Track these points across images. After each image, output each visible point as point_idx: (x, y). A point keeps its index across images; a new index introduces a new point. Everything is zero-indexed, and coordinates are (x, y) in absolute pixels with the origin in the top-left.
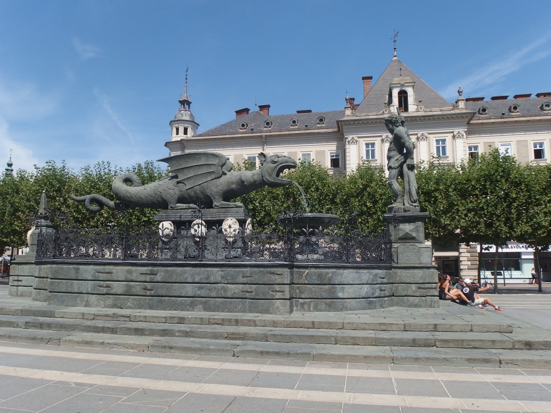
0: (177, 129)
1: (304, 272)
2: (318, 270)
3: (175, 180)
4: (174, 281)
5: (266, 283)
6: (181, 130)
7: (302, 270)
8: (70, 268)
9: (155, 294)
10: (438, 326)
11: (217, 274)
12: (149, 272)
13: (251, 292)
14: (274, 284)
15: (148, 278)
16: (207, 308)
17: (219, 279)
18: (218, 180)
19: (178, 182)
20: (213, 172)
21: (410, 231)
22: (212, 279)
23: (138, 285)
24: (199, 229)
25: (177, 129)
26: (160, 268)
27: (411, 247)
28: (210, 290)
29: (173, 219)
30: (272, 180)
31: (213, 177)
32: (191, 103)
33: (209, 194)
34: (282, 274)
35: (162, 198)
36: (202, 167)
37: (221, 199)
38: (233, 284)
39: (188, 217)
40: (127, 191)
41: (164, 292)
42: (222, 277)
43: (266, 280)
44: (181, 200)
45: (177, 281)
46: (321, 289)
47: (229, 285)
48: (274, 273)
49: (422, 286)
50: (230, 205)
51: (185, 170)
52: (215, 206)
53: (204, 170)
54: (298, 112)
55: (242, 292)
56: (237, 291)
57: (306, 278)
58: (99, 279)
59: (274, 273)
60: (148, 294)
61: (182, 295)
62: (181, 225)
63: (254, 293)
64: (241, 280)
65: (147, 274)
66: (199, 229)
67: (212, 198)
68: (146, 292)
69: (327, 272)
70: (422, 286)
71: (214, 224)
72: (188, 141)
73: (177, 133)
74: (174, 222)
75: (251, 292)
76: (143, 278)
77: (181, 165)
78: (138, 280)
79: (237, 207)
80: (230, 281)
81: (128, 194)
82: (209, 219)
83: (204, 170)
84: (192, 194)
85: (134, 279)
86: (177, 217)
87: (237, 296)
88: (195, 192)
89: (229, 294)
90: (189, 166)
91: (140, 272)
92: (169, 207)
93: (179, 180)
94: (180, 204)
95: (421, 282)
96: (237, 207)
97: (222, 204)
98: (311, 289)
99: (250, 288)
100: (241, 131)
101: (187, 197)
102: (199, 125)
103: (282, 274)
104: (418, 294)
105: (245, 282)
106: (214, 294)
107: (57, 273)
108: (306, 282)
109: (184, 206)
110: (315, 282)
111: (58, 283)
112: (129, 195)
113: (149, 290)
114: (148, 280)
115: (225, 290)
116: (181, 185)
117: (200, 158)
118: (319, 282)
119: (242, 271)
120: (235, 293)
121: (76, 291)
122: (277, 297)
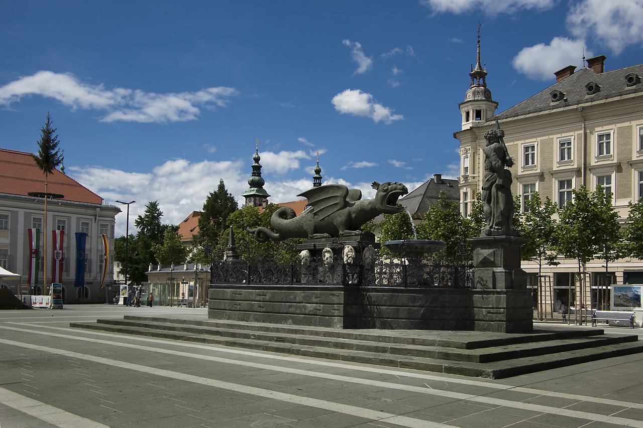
0: (468, 113)
4: (275, 301)
9: (266, 311)
10: (416, 340)
12: (261, 294)
13: (320, 310)
16: (295, 322)
21: (488, 255)
22: (297, 300)
25: (468, 113)
27: (486, 272)
28: (296, 307)
29: (309, 248)
32: (486, 74)
34: (339, 296)
37: (344, 228)
41: (269, 309)
42: (304, 298)
44: (317, 230)
48: (334, 295)
49: (492, 310)
50: (351, 233)
55: (315, 309)
56: (312, 309)
59: (334, 295)
60: (262, 311)
61: (281, 312)
62: (316, 253)
64: (314, 300)
65: (261, 295)
68: (260, 309)
70: (492, 310)
71: (337, 252)
73: (467, 120)
74: (310, 251)
75: (320, 310)
76: (258, 298)
78: (256, 300)
80: (308, 301)
87: (311, 313)
89: (307, 312)
92: (309, 237)
95: (490, 306)
100: (552, 104)
103: (339, 296)
104: (487, 318)
105: (318, 302)
106: (298, 311)
114: (261, 300)
115: (305, 308)
121: (223, 308)
122: (336, 314)
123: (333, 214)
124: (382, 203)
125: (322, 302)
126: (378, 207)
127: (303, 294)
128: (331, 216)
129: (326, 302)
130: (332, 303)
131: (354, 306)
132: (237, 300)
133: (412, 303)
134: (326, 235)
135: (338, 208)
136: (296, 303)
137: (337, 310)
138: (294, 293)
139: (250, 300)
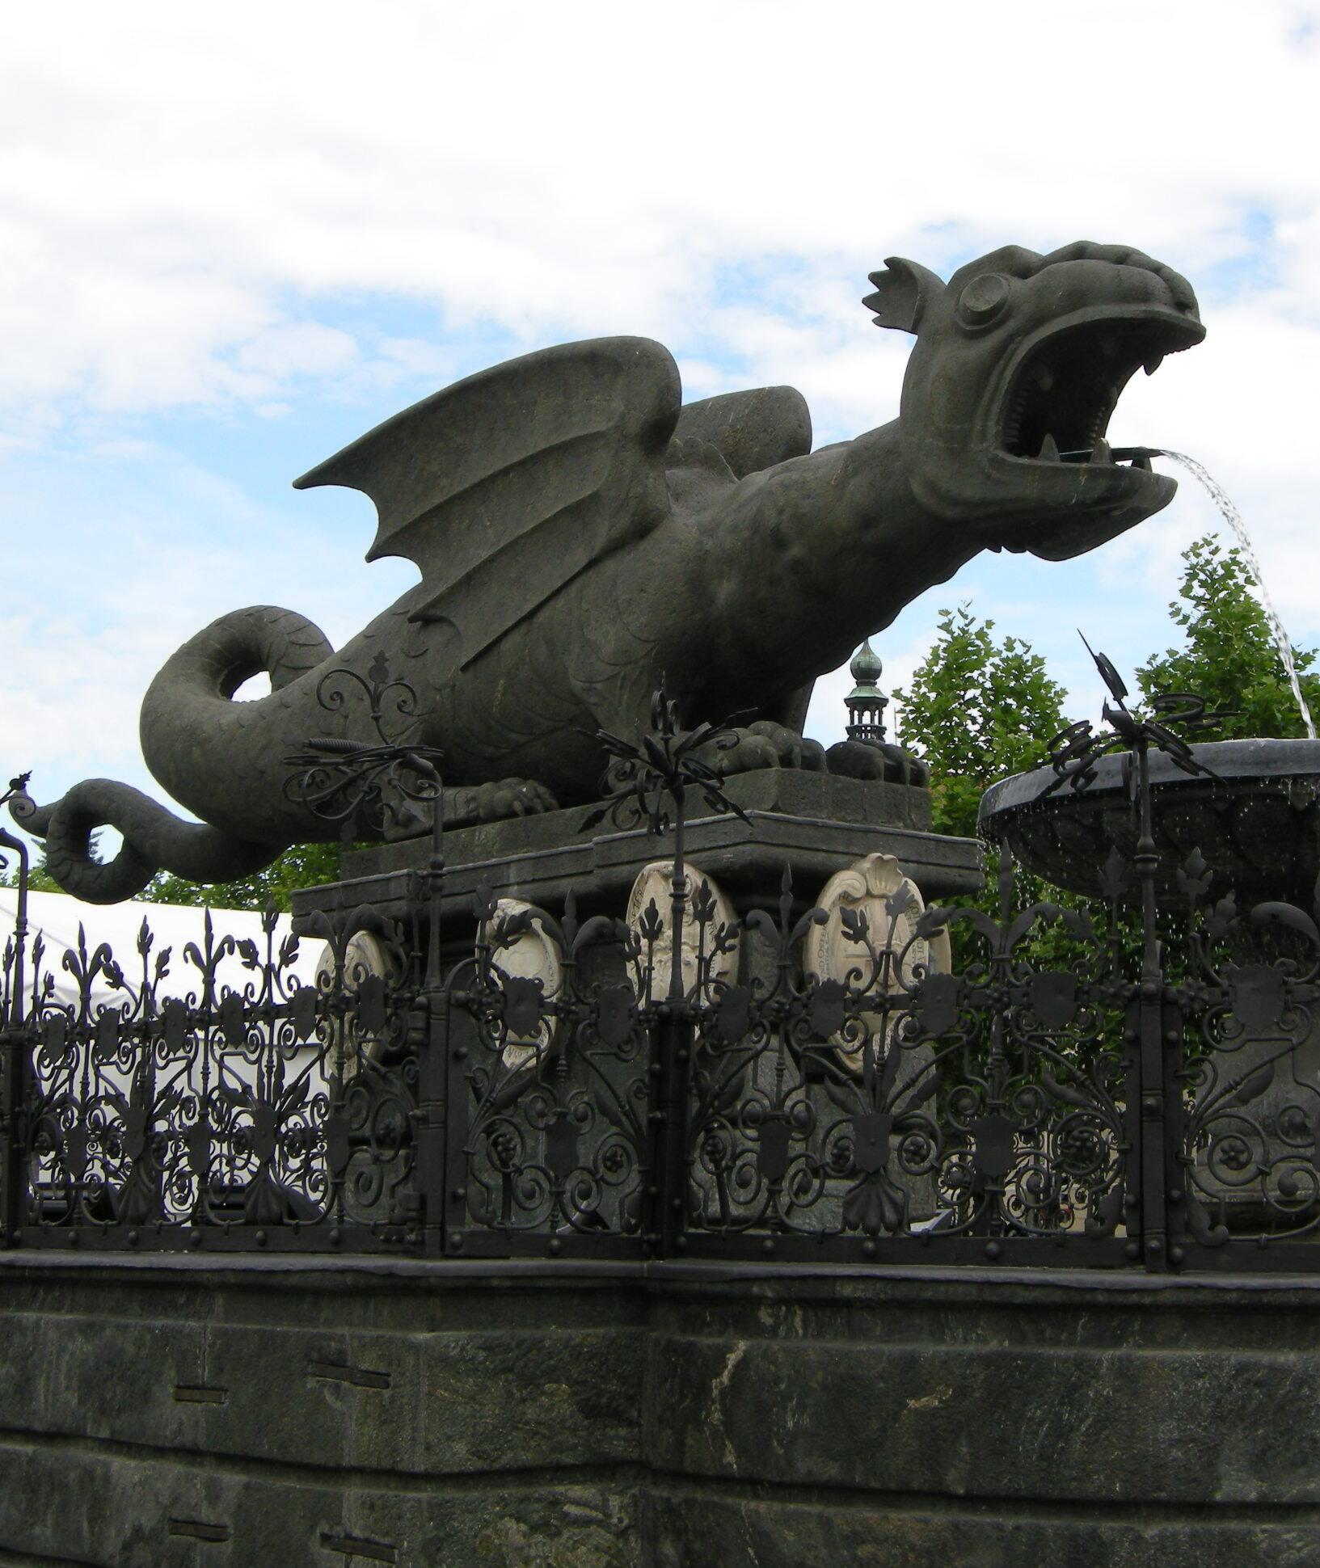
1: (720, 1355)
30: (971, 491)
33: (577, 685)
34: (376, 1379)
46: (855, 1539)
55: (177, 1525)
56: (148, 1519)
57: (729, 1423)
59: (334, 1364)
63: (228, 1547)
69: (911, 1362)
75: (216, 1535)
86: (394, 889)
99: (214, 1494)
110: (805, 1466)
116: (436, 637)
118: (831, 1471)
123: (560, 603)
124: (956, 445)
126: (931, 486)
127: (82, 1346)
128: (541, 618)
129: (265, 1449)
130: (318, 1457)
131: (578, 1495)
133: (1260, 1463)
135: (600, 543)
136: (29, 1435)
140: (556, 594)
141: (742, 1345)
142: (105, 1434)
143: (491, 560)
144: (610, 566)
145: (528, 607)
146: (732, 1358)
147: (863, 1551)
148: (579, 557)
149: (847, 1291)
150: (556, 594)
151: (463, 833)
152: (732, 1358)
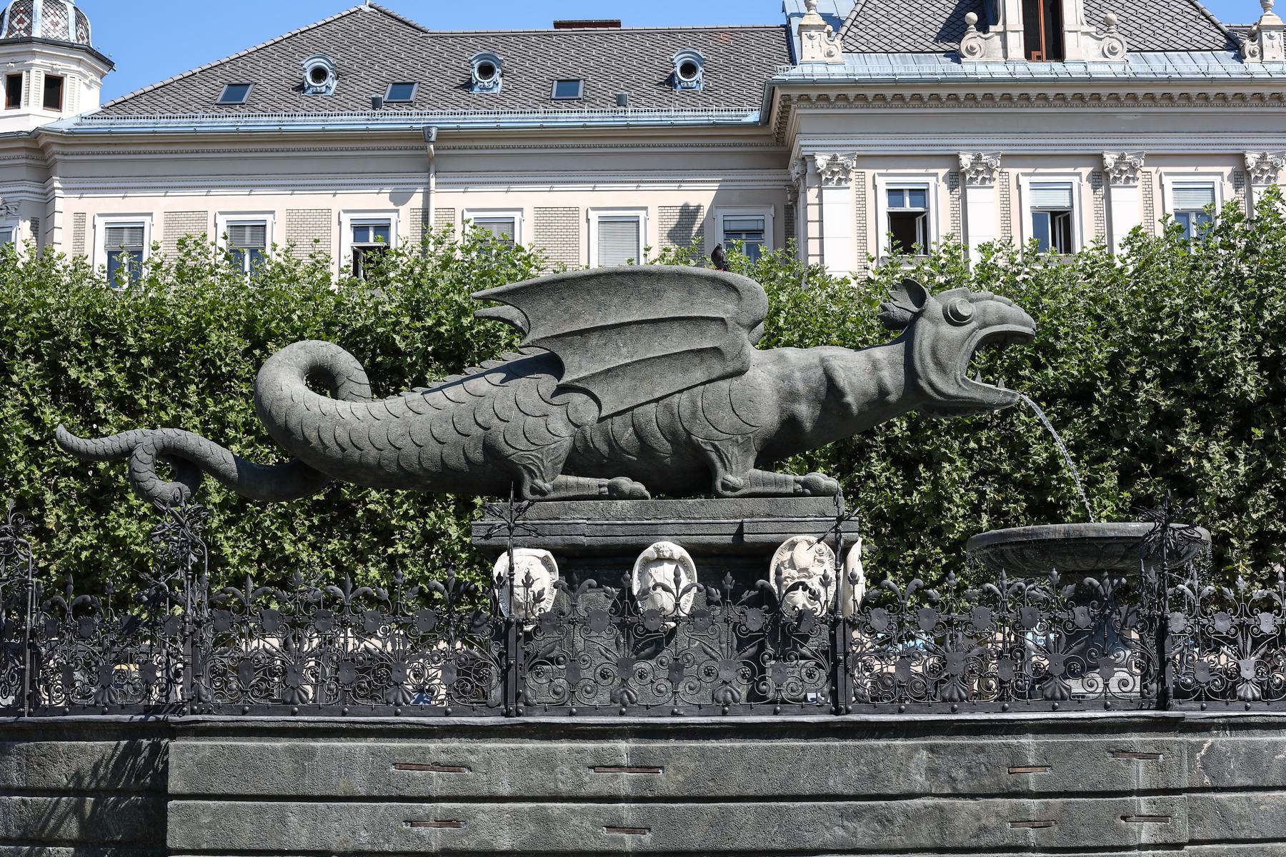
1: (1200, 745)
2: (1242, 738)
3: (548, 382)
4: (733, 791)
5: (1101, 788)
6: (34, 88)
7: (1195, 739)
8: (274, 751)
11: (912, 762)
12: (625, 761)
14: (1130, 793)
15: (624, 783)
17: (920, 780)
18: (736, 383)
19: (561, 390)
20: (716, 351)
23: (583, 813)
24: (667, 580)
26: (672, 743)
29: (558, 539)
30: (952, 390)
31: (718, 369)
33: (698, 439)
34: (1154, 756)
35: (490, 449)
36: (667, 326)
37: (751, 461)
38: (973, 796)
39: (619, 530)
40: (339, 421)
43: (1096, 778)
45: (751, 792)
46: (1258, 804)
47: (959, 802)
50: (786, 483)
51: (594, 340)
52: (725, 486)
53: (676, 342)
54: (558, 25)
57: (1205, 767)
58: (407, 792)
66: (667, 580)
67: (714, 456)
69: (1276, 744)
72: (74, 140)
76: (598, 783)
77: (575, 317)
79: (817, 491)
80: (961, 787)
81: (339, 431)
82: (707, 539)
83: (676, 342)
84: (626, 436)
85: (564, 789)
88: (638, 432)
90: (611, 322)
91: (590, 760)
92: (526, 492)
93: (567, 378)
94: (572, 479)
96: (817, 491)
97: (755, 481)
98: (1221, 806)
101: (604, 448)
102: (110, 64)
107: (212, 772)
108: (1207, 780)
109: (592, 483)
110: (1239, 782)
111: (214, 813)
112: (343, 438)
113: (632, 830)
117: (658, 294)
118: (1250, 782)
119: (1008, 746)
120: (984, 829)
122: (1145, 838)
123: (685, 395)
125: (1059, 787)
129: (1080, 787)
132: (429, 799)
134: (639, 486)
137: (1150, 818)
138: (873, 749)
139: (539, 792)
140: (681, 391)
141: (1210, 740)
142: (947, 790)
143: (627, 365)
144: (724, 385)
145: (657, 395)
146: (1206, 746)
147: (1262, 808)
148: (699, 375)
149: (1253, 719)
150: (681, 391)
151: (601, 503)
152: (1206, 746)
